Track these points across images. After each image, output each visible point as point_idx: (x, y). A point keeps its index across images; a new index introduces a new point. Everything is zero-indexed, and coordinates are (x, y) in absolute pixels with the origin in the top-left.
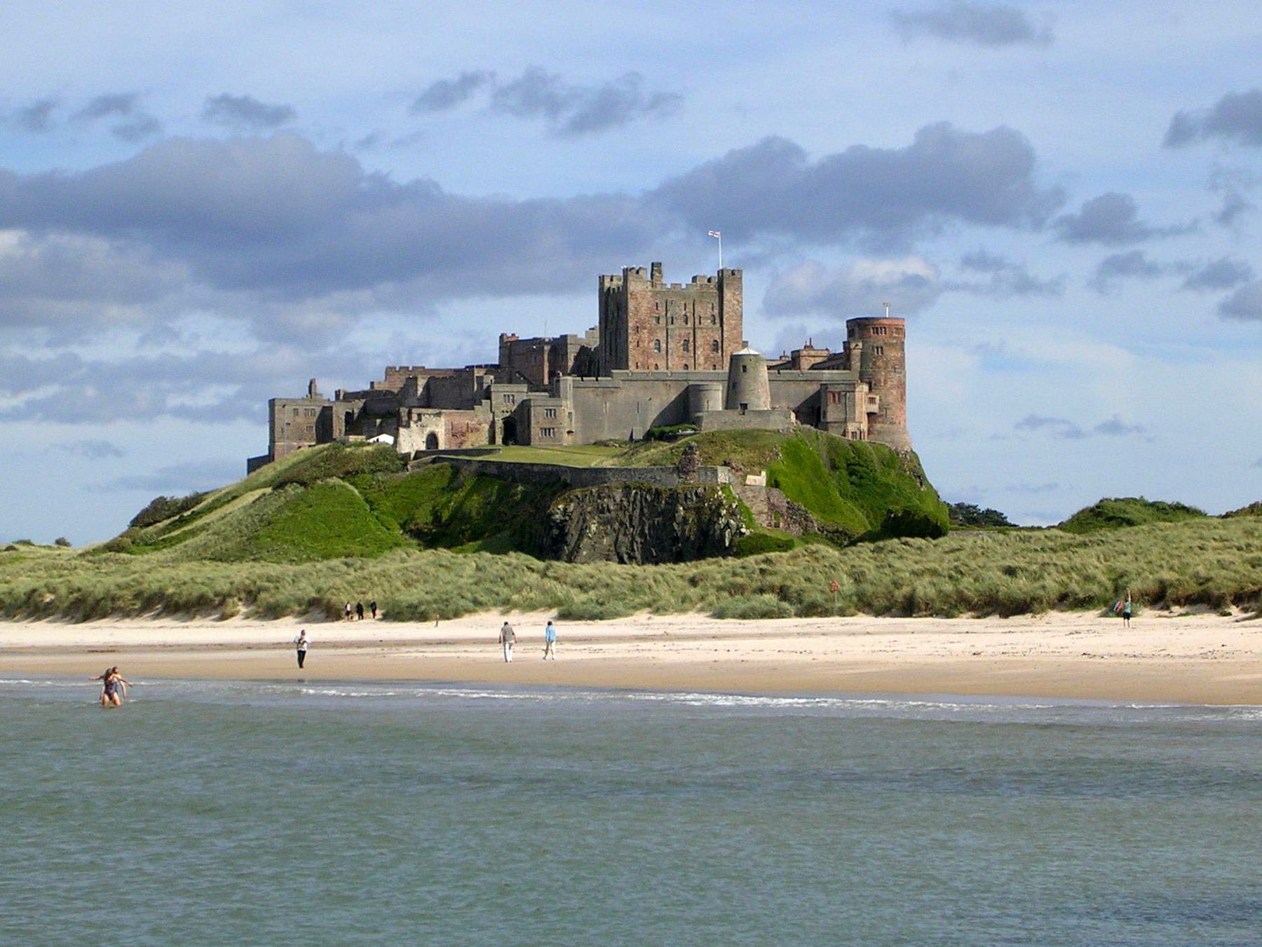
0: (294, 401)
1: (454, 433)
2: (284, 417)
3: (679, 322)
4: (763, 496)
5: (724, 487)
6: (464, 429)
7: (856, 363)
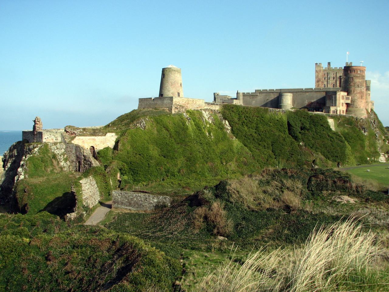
3: (331, 79)
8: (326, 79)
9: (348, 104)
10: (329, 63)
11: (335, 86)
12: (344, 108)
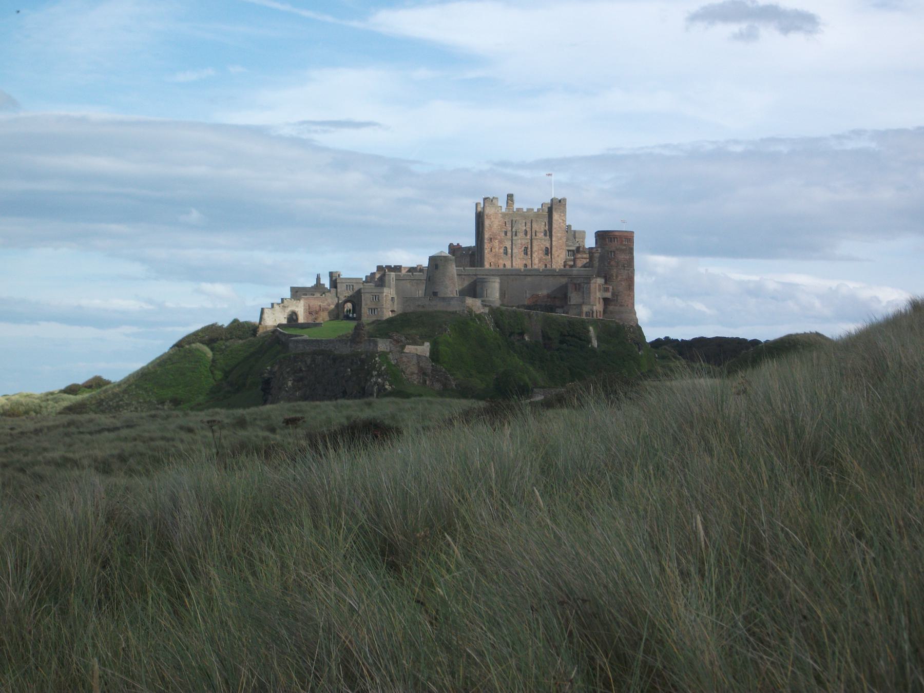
1: (310, 312)
3: (521, 234)
4: (415, 361)
5: (384, 355)
6: (318, 308)
8: (509, 234)
9: (606, 301)
10: (510, 197)
11: (529, 250)
12: (598, 307)
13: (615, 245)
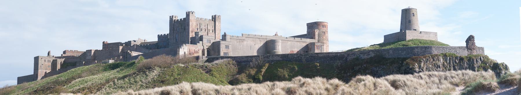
0: (45, 57)
2: (40, 62)
7: (317, 37)
13: (324, 29)
